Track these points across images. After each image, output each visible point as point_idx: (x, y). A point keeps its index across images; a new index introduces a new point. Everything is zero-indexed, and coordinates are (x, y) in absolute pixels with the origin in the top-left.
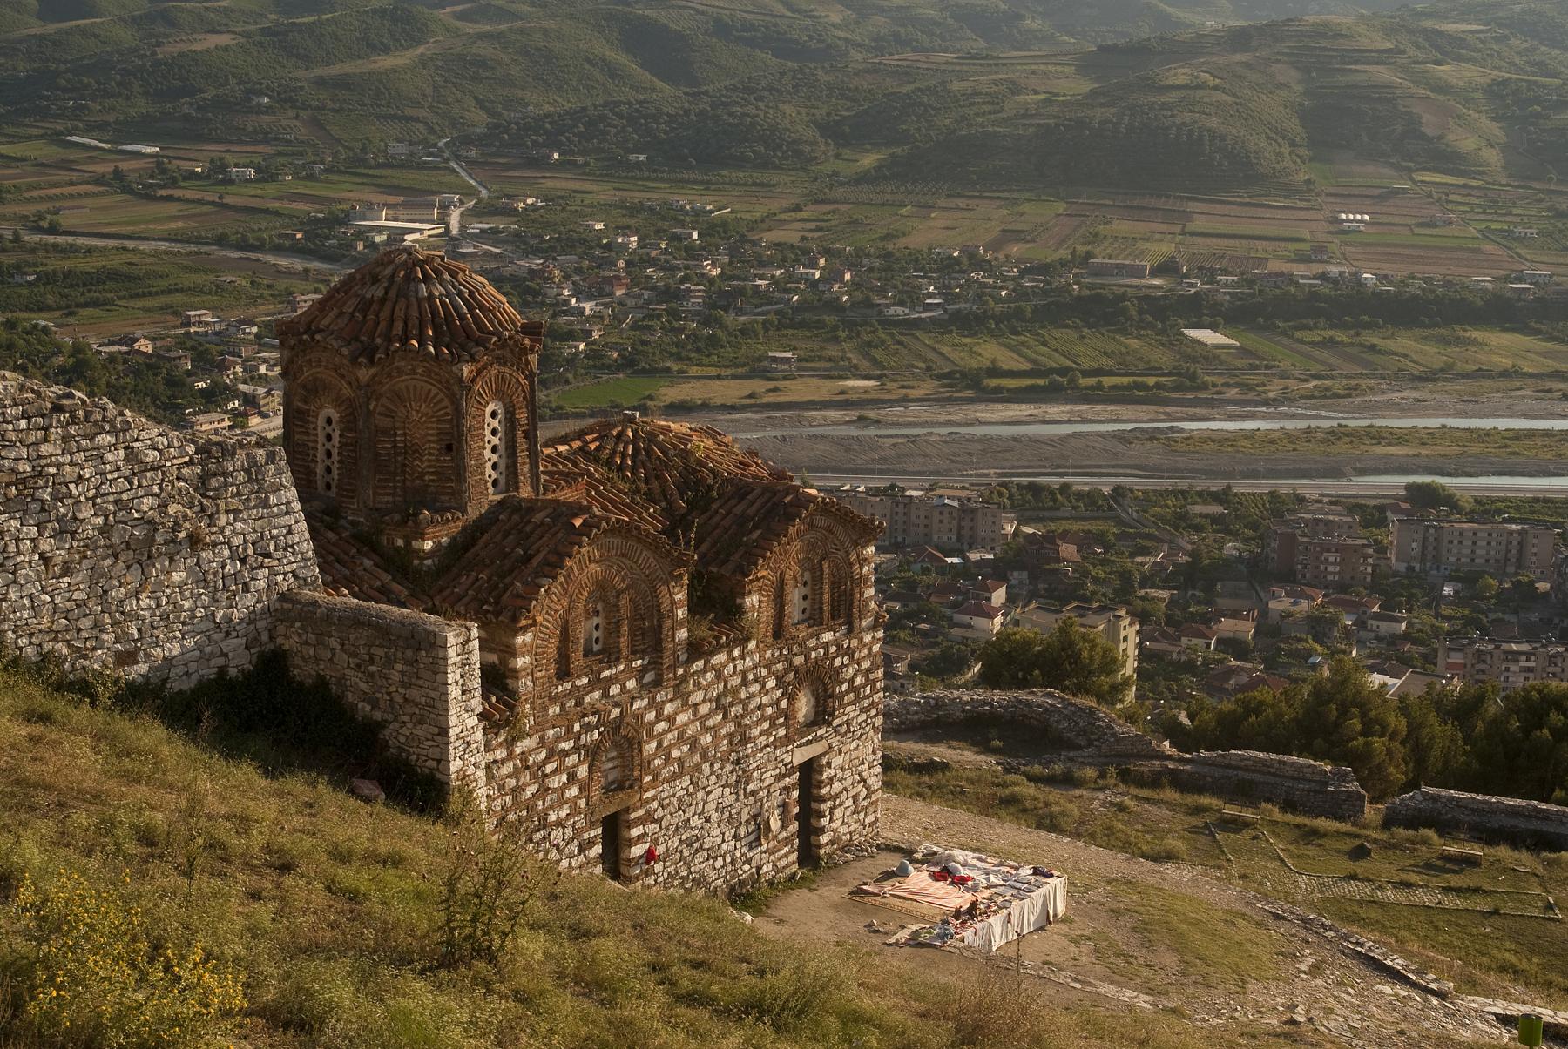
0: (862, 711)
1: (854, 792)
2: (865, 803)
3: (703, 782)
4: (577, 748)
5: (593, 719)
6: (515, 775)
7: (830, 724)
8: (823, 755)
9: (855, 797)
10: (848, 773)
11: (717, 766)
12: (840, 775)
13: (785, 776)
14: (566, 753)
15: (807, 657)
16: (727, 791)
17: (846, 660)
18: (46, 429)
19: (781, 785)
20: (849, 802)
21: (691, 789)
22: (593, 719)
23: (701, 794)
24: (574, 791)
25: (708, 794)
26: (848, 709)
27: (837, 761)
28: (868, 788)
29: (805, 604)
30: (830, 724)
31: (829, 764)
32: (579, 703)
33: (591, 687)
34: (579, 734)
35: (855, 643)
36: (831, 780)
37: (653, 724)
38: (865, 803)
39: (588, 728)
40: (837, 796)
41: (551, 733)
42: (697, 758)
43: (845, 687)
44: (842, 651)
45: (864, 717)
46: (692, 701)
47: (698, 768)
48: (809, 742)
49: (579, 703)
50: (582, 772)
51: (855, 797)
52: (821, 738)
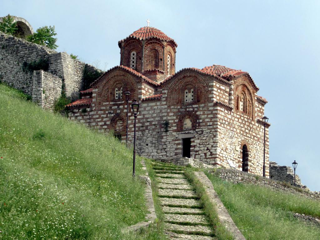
0: (208, 129)
1: (205, 152)
2: (210, 157)
3: (145, 134)
4: (107, 117)
5: (112, 112)
6: (90, 119)
7: (195, 130)
8: (193, 138)
9: (205, 154)
10: (202, 146)
11: (150, 132)
12: (199, 146)
13: (176, 140)
14: (103, 118)
15: (186, 109)
16: (154, 139)
17: (202, 113)
18: (26, 49)
19: (174, 142)
20: (203, 155)
21: (142, 136)
22: (112, 112)
23: (145, 138)
24: (106, 127)
25: (147, 138)
26: (201, 127)
27: (198, 141)
28: (211, 153)
29: (192, 98)
30: (195, 130)
31: (194, 141)
32: (111, 108)
33: (114, 105)
34: (108, 114)
35: (205, 109)
36: (194, 146)
37: (130, 116)
38: (210, 157)
39: (110, 113)
40: (197, 151)
41: (99, 112)
42: (144, 128)
43: (201, 121)
44: (198, 110)
45: (209, 131)
46: (143, 113)
47: (144, 130)
48: (187, 133)
49: (111, 108)
50: (108, 123)
51: (205, 154)
52: (191, 133)
